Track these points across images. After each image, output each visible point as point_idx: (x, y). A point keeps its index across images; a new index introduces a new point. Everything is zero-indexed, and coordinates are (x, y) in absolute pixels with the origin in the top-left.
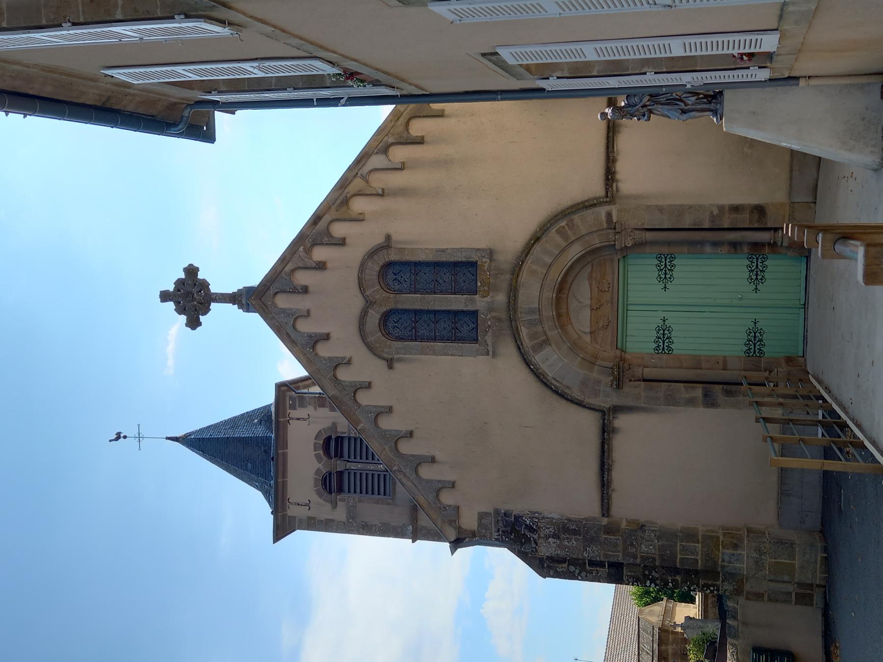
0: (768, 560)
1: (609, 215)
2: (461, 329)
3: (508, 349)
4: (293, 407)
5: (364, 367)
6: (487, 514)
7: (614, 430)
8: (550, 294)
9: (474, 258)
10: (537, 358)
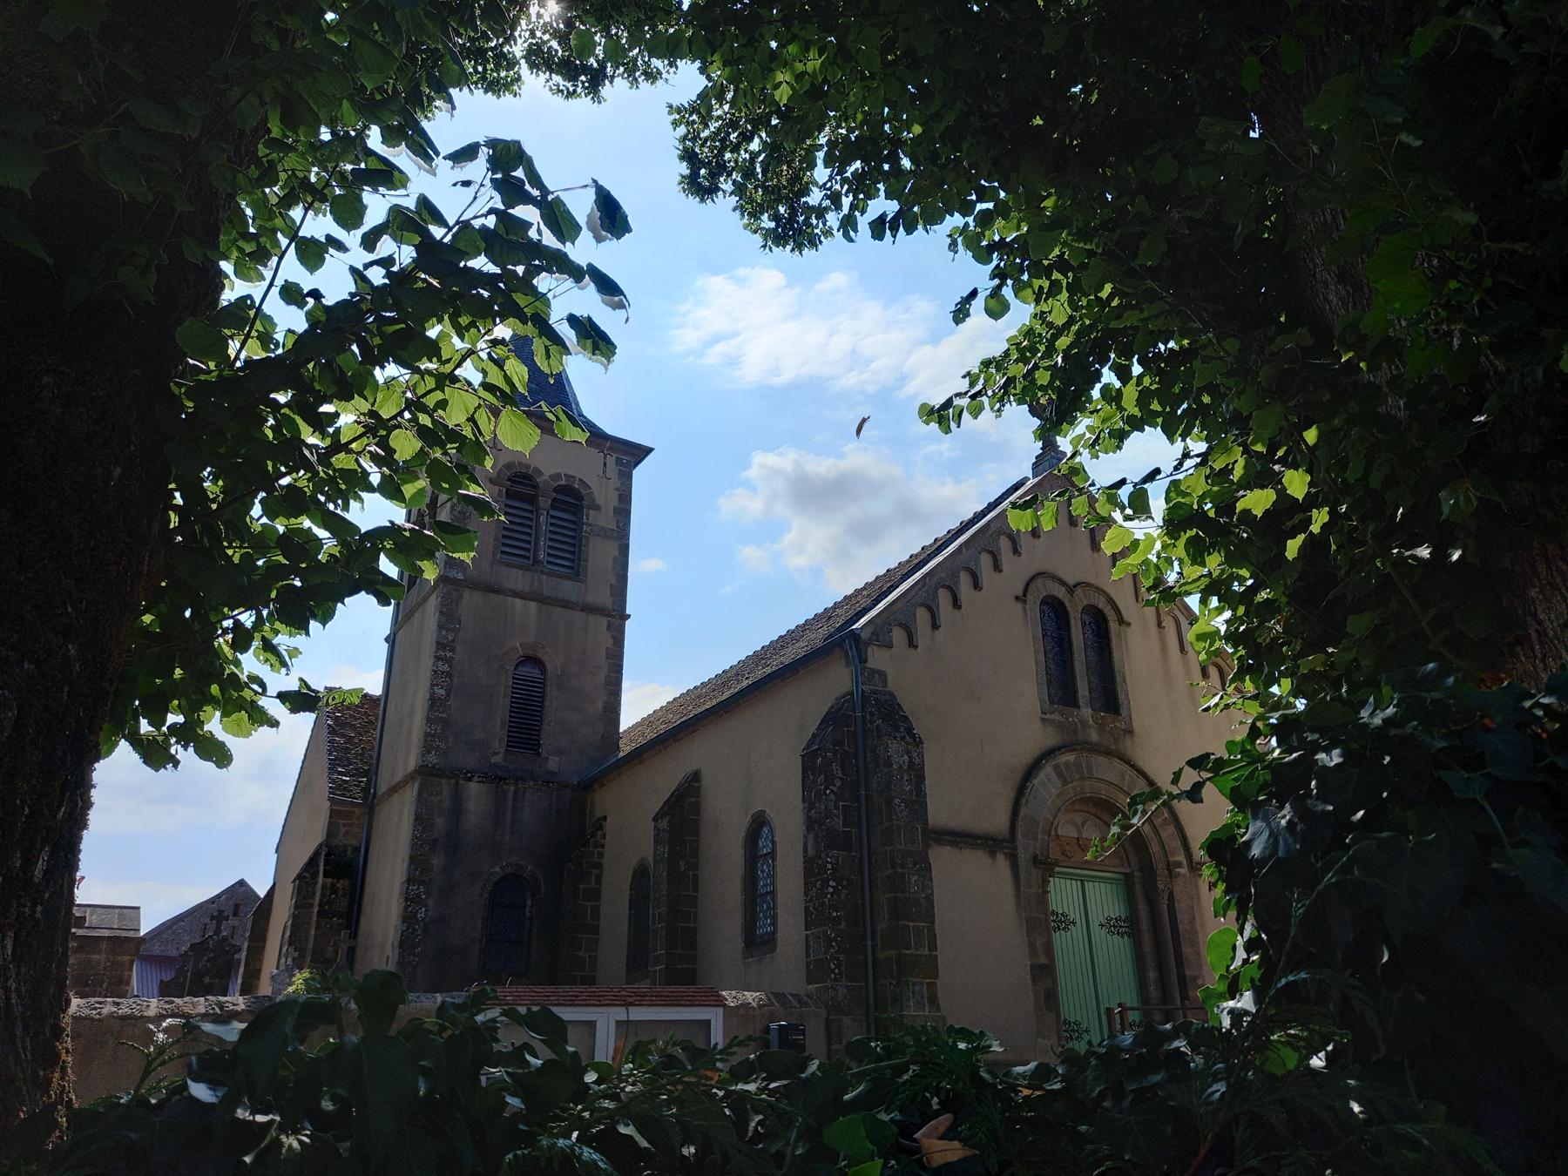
0: (909, 1040)
1: (1179, 865)
2: (1061, 689)
3: (1049, 738)
4: (619, 462)
5: (1016, 571)
6: (885, 682)
7: (992, 854)
8: (1104, 792)
9: (1124, 712)
10: (1048, 769)
